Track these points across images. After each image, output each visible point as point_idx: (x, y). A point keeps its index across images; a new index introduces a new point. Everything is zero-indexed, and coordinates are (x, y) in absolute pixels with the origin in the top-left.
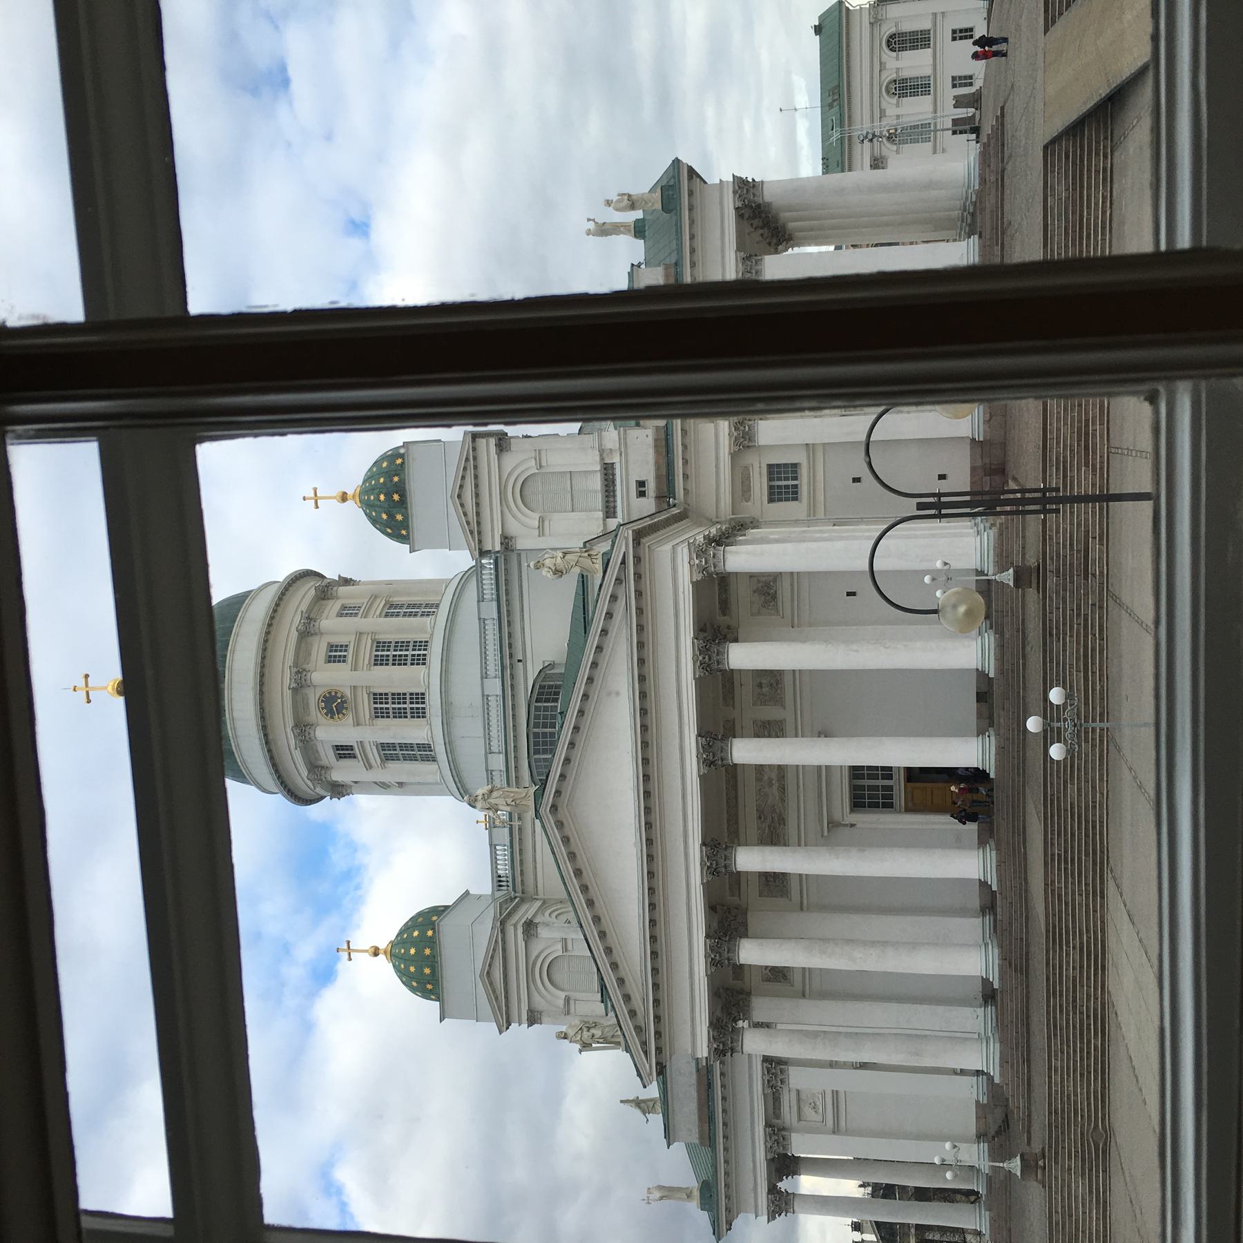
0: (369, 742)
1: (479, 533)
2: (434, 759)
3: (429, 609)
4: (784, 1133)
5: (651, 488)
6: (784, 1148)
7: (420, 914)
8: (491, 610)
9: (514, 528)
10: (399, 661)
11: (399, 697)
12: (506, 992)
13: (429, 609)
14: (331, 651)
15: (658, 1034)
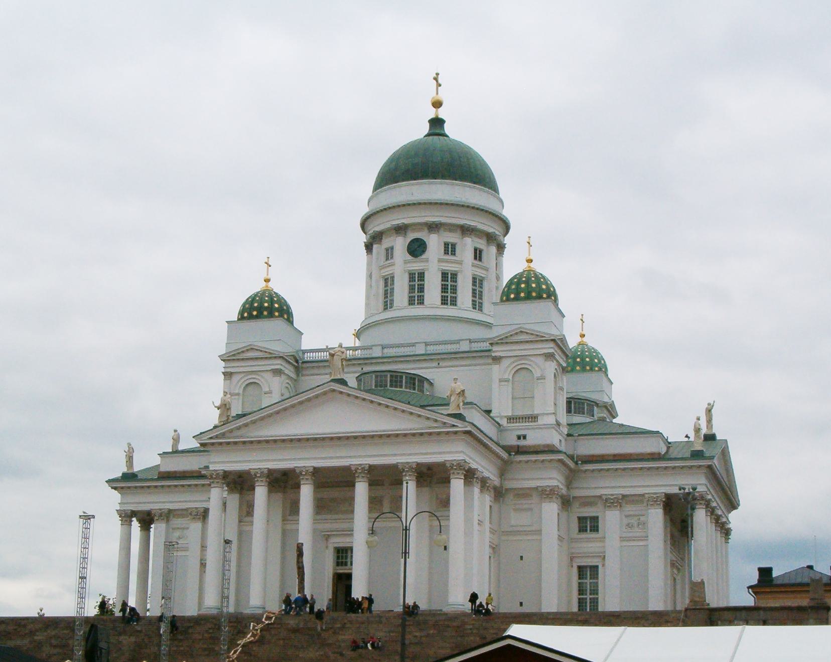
0: (394, 270)
1: (502, 343)
2: (385, 309)
3: (477, 305)
4: (165, 520)
5: (522, 443)
6: (157, 520)
7: (288, 307)
8: (465, 347)
9: (505, 363)
10: (444, 289)
11: (421, 289)
12: (243, 359)
13: (477, 305)
14: (452, 245)
15: (221, 444)
